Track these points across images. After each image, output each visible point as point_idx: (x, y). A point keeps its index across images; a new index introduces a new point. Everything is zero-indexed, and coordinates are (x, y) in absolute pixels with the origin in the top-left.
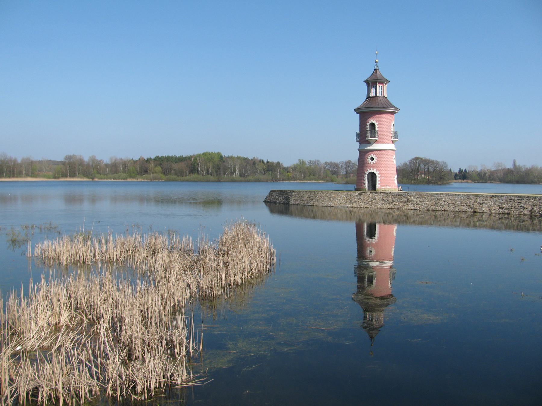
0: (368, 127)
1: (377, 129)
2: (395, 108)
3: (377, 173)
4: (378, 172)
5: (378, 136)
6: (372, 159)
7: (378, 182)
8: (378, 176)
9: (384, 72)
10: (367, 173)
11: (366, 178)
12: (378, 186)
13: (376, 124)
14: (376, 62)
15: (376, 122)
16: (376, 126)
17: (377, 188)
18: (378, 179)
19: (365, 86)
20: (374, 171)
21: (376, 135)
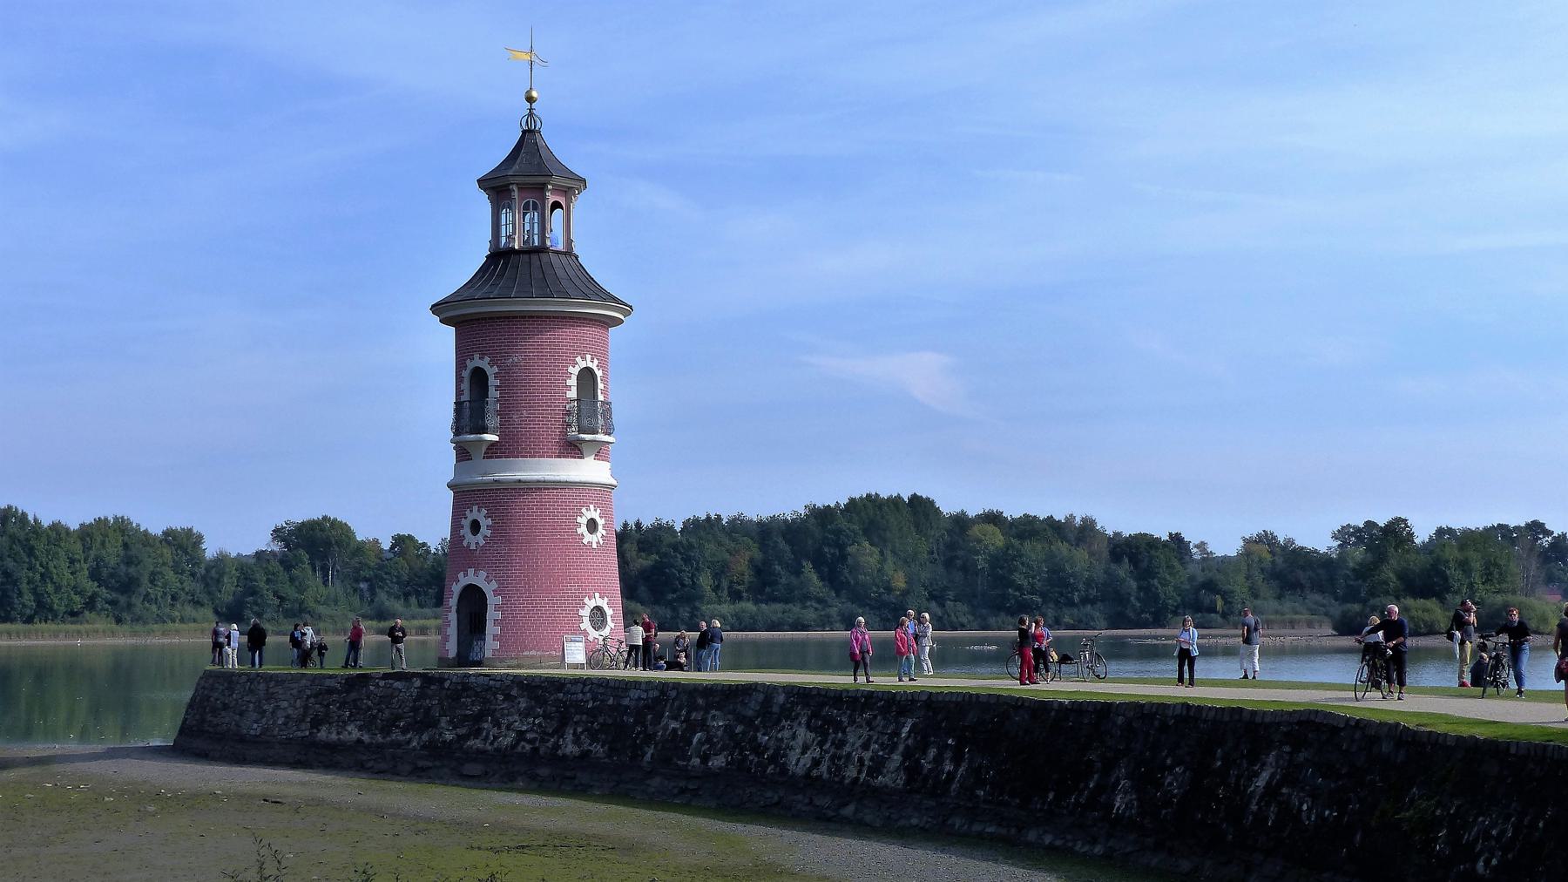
3: (489, 589)
4: (494, 585)
6: (475, 527)
7: (491, 629)
8: (492, 600)
9: (562, 148)
10: (456, 589)
12: (491, 646)
13: (491, 371)
14: (530, 99)
16: (493, 382)
17: (488, 654)
18: (492, 614)
19: (482, 204)
20: (478, 579)
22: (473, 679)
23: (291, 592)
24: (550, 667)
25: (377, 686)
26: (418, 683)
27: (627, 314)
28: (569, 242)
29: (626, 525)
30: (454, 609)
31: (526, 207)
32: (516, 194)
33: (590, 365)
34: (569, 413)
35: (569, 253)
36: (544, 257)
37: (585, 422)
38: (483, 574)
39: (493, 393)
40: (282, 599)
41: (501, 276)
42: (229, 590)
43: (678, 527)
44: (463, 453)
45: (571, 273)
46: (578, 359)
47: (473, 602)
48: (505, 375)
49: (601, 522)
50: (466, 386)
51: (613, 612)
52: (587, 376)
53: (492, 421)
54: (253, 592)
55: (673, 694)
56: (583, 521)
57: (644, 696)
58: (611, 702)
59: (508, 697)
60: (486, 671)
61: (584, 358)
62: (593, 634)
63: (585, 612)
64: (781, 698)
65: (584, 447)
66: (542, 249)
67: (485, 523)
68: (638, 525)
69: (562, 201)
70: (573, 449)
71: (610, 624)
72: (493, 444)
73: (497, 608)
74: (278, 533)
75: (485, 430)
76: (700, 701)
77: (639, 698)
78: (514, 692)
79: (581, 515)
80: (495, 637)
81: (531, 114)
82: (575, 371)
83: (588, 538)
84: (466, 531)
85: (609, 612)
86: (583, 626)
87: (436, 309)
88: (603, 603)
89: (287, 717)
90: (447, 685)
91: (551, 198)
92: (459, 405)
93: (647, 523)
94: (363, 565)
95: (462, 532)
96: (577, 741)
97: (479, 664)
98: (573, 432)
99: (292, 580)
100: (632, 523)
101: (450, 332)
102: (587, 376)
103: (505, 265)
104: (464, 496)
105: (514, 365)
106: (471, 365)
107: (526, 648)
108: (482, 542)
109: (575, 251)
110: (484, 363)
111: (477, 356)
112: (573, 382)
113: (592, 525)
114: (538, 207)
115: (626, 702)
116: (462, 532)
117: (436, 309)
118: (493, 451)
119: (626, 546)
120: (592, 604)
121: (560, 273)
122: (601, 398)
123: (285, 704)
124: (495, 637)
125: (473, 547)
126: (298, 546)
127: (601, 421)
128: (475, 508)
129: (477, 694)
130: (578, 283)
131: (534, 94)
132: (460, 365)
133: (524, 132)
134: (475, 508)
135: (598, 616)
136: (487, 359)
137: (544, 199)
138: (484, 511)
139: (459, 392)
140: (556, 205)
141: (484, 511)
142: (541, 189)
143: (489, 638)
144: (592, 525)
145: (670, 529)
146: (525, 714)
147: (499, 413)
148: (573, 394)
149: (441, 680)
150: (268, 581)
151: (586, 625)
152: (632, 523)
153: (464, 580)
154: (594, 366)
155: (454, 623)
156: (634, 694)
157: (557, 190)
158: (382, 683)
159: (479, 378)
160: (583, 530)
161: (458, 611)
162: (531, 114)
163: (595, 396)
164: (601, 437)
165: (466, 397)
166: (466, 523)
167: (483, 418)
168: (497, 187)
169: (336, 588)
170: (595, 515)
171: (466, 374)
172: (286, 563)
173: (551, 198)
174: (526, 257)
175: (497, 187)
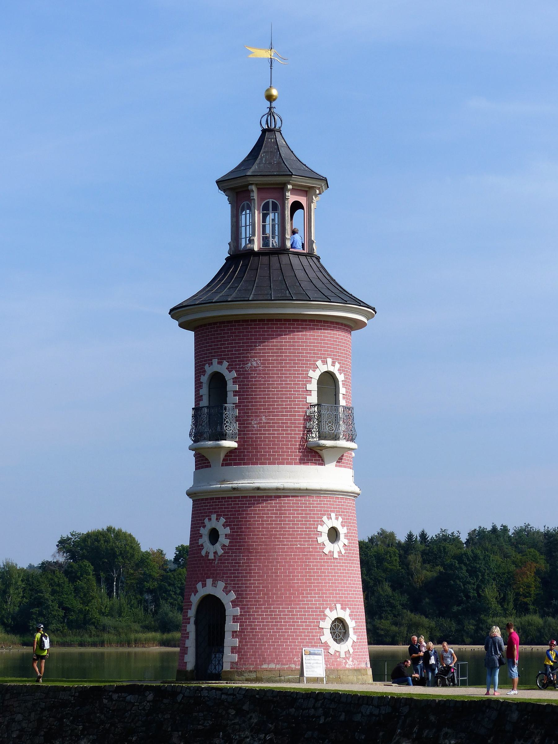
2: (359, 302)
3: (228, 599)
4: (233, 596)
6: (214, 536)
7: (230, 641)
8: (231, 611)
9: (302, 144)
10: (195, 599)
12: (229, 658)
13: (230, 376)
14: (270, 98)
15: (230, 370)
16: (232, 387)
17: (227, 667)
18: (231, 626)
20: (217, 590)
22: (205, 693)
23: (77, 604)
24: (289, 681)
25: (110, 699)
26: (150, 697)
27: (370, 316)
28: (311, 242)
29: (410, 536)
30: (192, 620)
31: (266, 208)
32: (255, 195)
33: (331, 369)
34: (308, 419)
35: (310, 255)
36: (284, 259)
37: (326, 429)
38: (221, 585)
39: (232, 399)
40: (66, 609)
41: (240, 278)
42: (14, 601)
43: (464, 538)
44: (202, 461)
45: (312, 275)
46: (319, 363)
47: (212, 610)
48: (243, 379)
49: (342, 531)
50: (204, 391)
51: (357, 625)
52: (328, 381)
53: (232, 427)
54: (39, 602)
55: (406, 710)
56: (324, 529)
57: (376, 712)
58: (343, 717)
60: (223, 684)
61: (325, 362)
62: (334, 646)
63: (326, 624)
64: (515, 716)
65: (324, 453)
66: (282, 251)
67: (224, 531)
68: (423, 535)
69: (303, 200)
70: (313, 455)
71: (352, 636)
72: (232, 451)
73: (236, 619)
74: (63, 544)
75: (223, 437)
76: (432, 718)
77: (371, 714)
78: (245, 707)
79: (322, 523)
80: (234, 650)
81: (271, 113)
82: (315, 375)
83: (329, 547)
84: (205, 540)
85: (351, 624)
86: (324, 639)
87: (175, 312)
88: (345, 615)
90: (179, 698)
91: (291, 198)
92: (197, 410)
93: (432, 533)
94: (148, 577)
95: (201, 541)
97: (218, 677)
98: (314, 438)
99: (77, 590)
100: (416, 533)
101: (188, 337)
102: (328, 381)
103: (245, 266)
104: (204, 505)
105: (254, 369)
106: (209, 370)
107: (264, 661)
108: (220, 552)
109: (316, 252)
110: (223, 369)
111: (215, 361)
112: (313, 386)
113: (334, 534)
114: (278, 207)
115: (358, 718)
116: (201, 541)
117: (175, 312)
118: (233, 458)
119: (411, 557)
120: (332, 615)
121: (300, 274)
122: (342, 402)
123: (19, 717)
124: (234, 650)
125: (211, 556)
126: (83, 557)
127: (343, 427)
128: (214, 517)
130: (319, 285)
131: (274, 92)
132: (199, 370)
133: (264, 131)
134: (214, 517)
135: (340, 629)
136: (226, 364)
137: (284, 199)
138: (223, 520)
139: (198, 398)
140: (297, 206)
141: (223, 520)
142: (281, 189)
143: (227, 651)
144: (334, 534)
145: (455, 540)
147: (238, 419)
148: (313, 399)
149: (174, 693)
150: (53, 592)
151: (327, 637)
152: (416, 533)
153: (202, 591)
154: (335, 369)
156: (367, 710)
157: (297, 190)
158: (115, 696)
159: (218, 381)
160: (324, 538)
161: (196, 623)
162: (271, 113)
163: (337, 401)
164: (342, 443)
165: (205, 402)
166: (205, 532)
167: (221, 424)
168: (237, 188)
169: (119, 599)
170: (337, 524)
171: (204, 379)
172: (70, 573)
173: (291, 198)
174: (264, 259)
175: (237, 188)
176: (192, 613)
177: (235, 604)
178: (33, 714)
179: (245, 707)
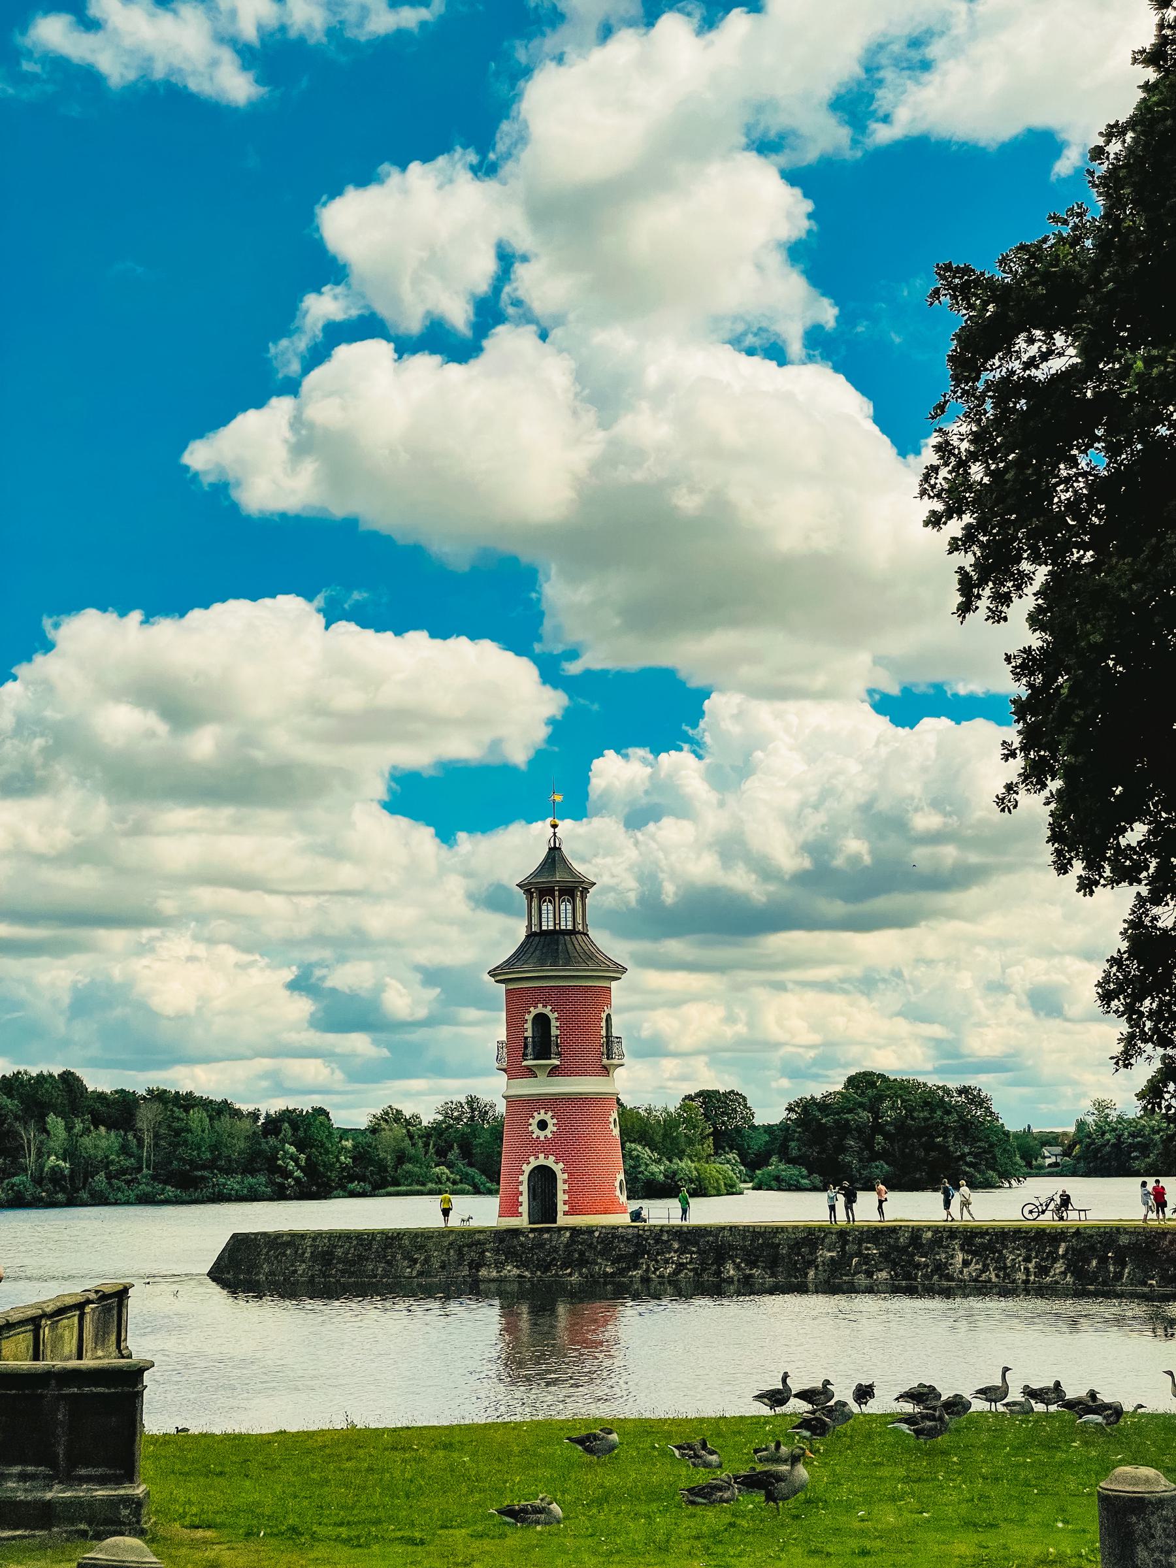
0: (529, 1025)
1: (554, 1032)
3: (558, 1168)
5: (559, 1054)
6: (543, 1125)
8: (561, 1177)
10: (527, 1169)
11: (524, 1188)
13: (553, 1016)
16: (554, 1023)
18: (561, 1186)
20: (550, 1162)
21: (554, 1049)
26: (568, 1234)
59: (658, 1240)
89: (443, 1262)
90: (597, 1234)
96: (737, 1267)
106: (534, 1011)
110: (547, 1011)
118: (554, 1071)
129: (628, 1241)
146: (681, 1252)
153: (534, 1163)
155: (525, 1194)
159: (542, 1022)
176: (524, 1178)
177: (564, 1171)
178: (452, 1252)
179: (665, 1238)
